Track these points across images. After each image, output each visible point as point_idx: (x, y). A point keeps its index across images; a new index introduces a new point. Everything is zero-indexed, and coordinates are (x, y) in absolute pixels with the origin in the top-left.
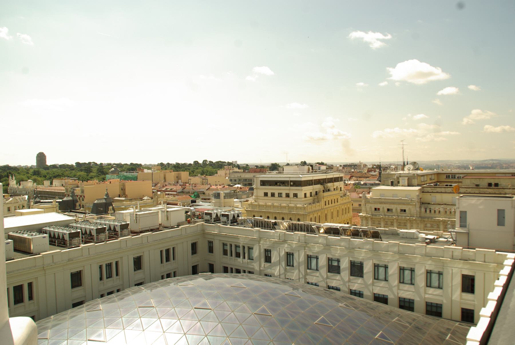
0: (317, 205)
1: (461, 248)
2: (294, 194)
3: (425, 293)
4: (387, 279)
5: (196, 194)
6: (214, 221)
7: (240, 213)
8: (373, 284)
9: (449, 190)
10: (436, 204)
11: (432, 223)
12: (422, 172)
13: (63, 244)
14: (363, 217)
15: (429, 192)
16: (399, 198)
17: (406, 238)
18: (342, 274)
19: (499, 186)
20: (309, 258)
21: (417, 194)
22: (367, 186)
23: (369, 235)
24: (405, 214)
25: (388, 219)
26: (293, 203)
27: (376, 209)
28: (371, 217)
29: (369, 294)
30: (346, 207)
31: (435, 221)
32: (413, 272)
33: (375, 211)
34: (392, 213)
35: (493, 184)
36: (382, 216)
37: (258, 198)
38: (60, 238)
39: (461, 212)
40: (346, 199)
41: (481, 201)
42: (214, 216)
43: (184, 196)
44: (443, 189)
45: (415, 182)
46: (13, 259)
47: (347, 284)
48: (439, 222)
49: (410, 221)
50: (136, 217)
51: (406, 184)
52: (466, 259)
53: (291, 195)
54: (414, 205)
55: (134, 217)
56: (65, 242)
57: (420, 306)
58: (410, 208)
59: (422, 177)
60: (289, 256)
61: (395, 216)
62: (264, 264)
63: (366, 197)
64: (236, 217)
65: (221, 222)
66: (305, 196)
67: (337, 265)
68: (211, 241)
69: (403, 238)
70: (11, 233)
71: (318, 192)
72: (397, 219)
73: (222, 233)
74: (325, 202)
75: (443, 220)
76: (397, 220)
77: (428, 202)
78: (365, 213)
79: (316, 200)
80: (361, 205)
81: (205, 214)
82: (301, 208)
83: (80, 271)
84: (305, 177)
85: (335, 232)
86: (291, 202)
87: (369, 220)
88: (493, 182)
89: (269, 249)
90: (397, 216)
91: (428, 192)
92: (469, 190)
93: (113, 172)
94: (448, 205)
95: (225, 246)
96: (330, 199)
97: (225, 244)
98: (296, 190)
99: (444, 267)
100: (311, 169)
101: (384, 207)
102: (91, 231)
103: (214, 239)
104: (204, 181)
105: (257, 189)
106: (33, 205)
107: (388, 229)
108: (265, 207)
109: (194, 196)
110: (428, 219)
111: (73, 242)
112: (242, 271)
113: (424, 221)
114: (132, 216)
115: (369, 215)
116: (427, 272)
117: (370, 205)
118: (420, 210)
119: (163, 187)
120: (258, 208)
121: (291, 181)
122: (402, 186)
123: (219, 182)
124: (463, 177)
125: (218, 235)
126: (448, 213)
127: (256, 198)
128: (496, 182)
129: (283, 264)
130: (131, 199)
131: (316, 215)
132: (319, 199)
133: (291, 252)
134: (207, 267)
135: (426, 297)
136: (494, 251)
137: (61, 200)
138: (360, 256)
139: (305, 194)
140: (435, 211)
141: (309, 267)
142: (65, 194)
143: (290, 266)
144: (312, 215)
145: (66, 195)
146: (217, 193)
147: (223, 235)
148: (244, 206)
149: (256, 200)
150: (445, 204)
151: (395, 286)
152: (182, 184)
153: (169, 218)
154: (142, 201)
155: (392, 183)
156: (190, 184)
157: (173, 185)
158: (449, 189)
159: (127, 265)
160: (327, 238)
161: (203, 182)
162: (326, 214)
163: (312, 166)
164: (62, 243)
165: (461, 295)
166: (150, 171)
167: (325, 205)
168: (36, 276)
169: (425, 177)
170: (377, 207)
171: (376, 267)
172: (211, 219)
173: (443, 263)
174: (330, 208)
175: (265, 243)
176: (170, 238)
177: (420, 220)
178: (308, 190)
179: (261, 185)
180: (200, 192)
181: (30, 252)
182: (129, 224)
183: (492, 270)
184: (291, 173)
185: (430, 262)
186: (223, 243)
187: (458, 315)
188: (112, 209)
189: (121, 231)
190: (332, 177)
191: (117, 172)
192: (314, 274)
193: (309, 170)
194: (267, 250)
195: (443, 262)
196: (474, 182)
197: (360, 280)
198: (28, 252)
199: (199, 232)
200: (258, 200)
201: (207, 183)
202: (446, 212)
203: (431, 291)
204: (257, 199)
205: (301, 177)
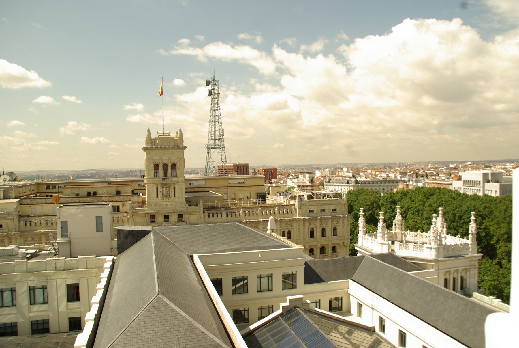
1: (64, 258)
3: (30, 312)
9: (50, 200)
10: (37, 216)
11: (33, 236)
12: (19, 182)
15: (29, 203)
17: (4, 256)
21: (15, 206)
24: (2, 229)
31: (36, 234)
35: (92, 192)
41: (80, 210)
44: (43, 200)
45: (12, 193)
48: (41, 234)
49: (8, 237)
52: (69, 269)
54: (12, 219)
58: (7, 223)
59: (21, 189)
75: (44, 232)
88: (92, 191)
92: (70, 200)
94: (49, 216)
110: (28, 232)
116: (30, 289)
126: (50, 224)
135: (30, 315)
136: (95, 256)
140: (36, 223)
150: (46, 216)
165: (67, 306)
169: (24, 188)
173: (47, 277)
177: (19, 234)
183: (94, 275)
185: (32, 278)
187: (65, 325)
195: (47, 276)
196: (74, 191)
202: (47, 223)
203: (35, 308)
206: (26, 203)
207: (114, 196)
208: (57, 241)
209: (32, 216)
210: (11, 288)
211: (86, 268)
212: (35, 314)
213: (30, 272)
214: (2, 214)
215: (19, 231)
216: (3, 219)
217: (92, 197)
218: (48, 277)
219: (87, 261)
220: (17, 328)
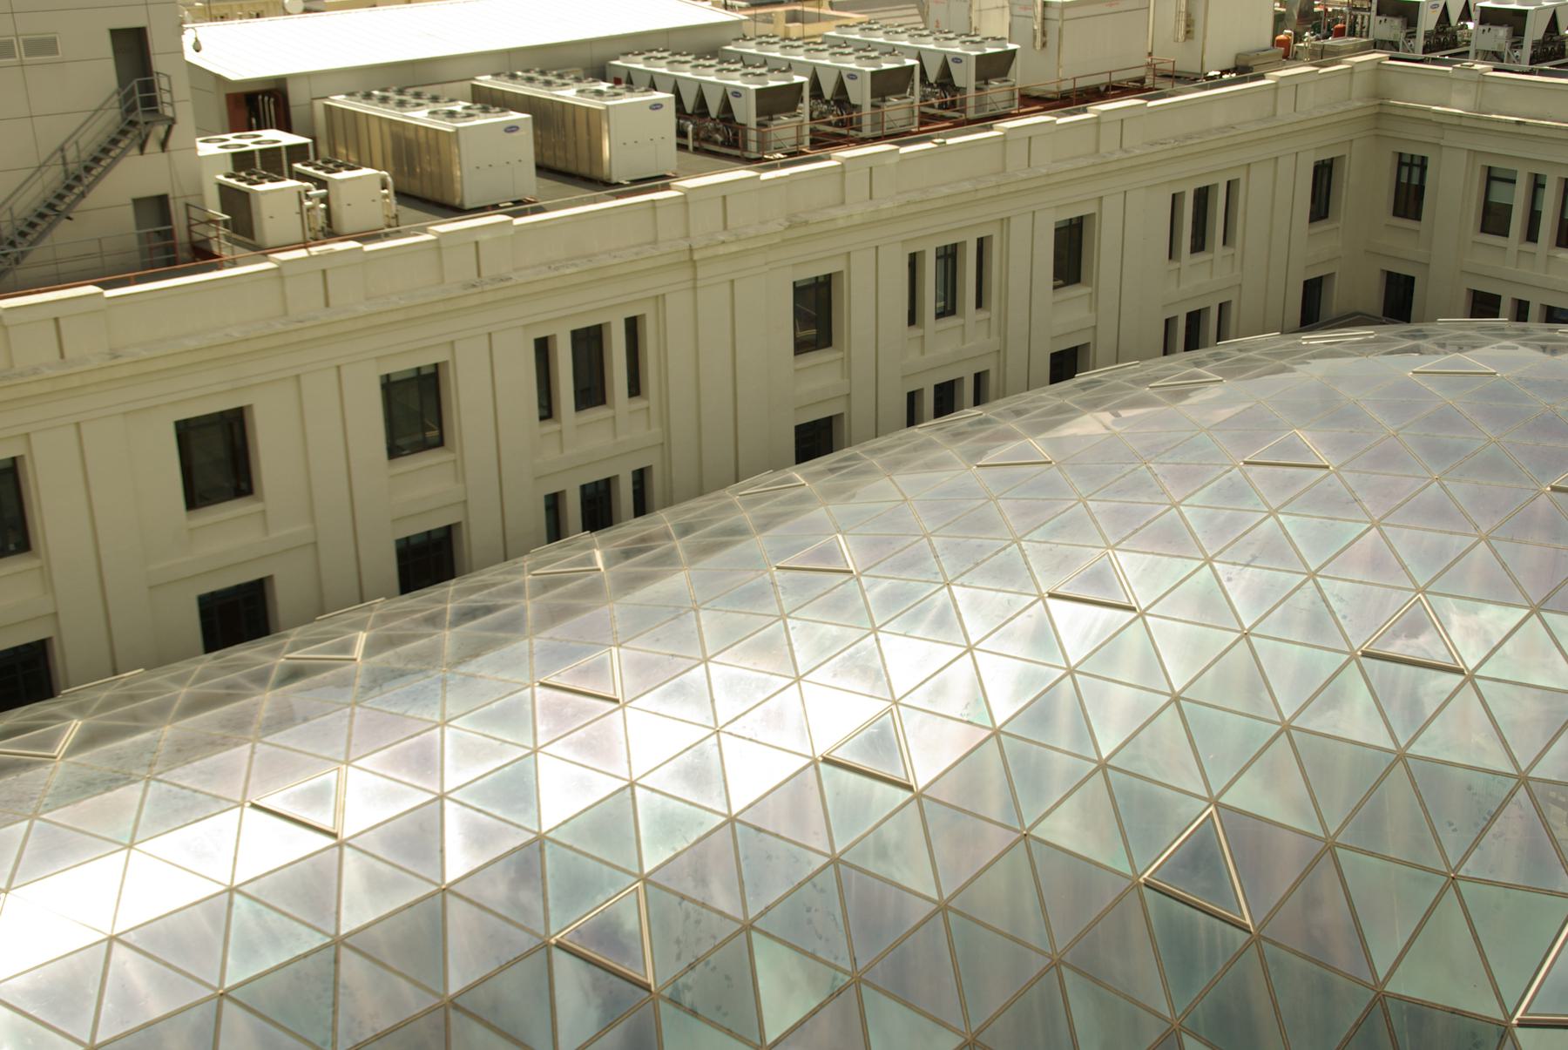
13: (723, 144)
46: (540, 210)
50: (1044, 19)
55: (1036, 17)
56: (735, 134)
65: (1472, 53)
68: (1412, 156)
70: (486, 81)
73: (1494, 116)
83: (829, 277)
95: (1497, 187)
97: (1495, 174)
102: (847, 82)
103: (1441, 146)
111: (773, 138)
114: (1017, 11)
125: (1464, 122)
134: (1373, 296)
153: (1198, 29)
164: (719, 138)
168: (660, 292)
176: (1220, 129)
181: (596, 174)
182: (1014, 52)
186: (1490, 168)
198: (596, 182)
199: (1359, 104)
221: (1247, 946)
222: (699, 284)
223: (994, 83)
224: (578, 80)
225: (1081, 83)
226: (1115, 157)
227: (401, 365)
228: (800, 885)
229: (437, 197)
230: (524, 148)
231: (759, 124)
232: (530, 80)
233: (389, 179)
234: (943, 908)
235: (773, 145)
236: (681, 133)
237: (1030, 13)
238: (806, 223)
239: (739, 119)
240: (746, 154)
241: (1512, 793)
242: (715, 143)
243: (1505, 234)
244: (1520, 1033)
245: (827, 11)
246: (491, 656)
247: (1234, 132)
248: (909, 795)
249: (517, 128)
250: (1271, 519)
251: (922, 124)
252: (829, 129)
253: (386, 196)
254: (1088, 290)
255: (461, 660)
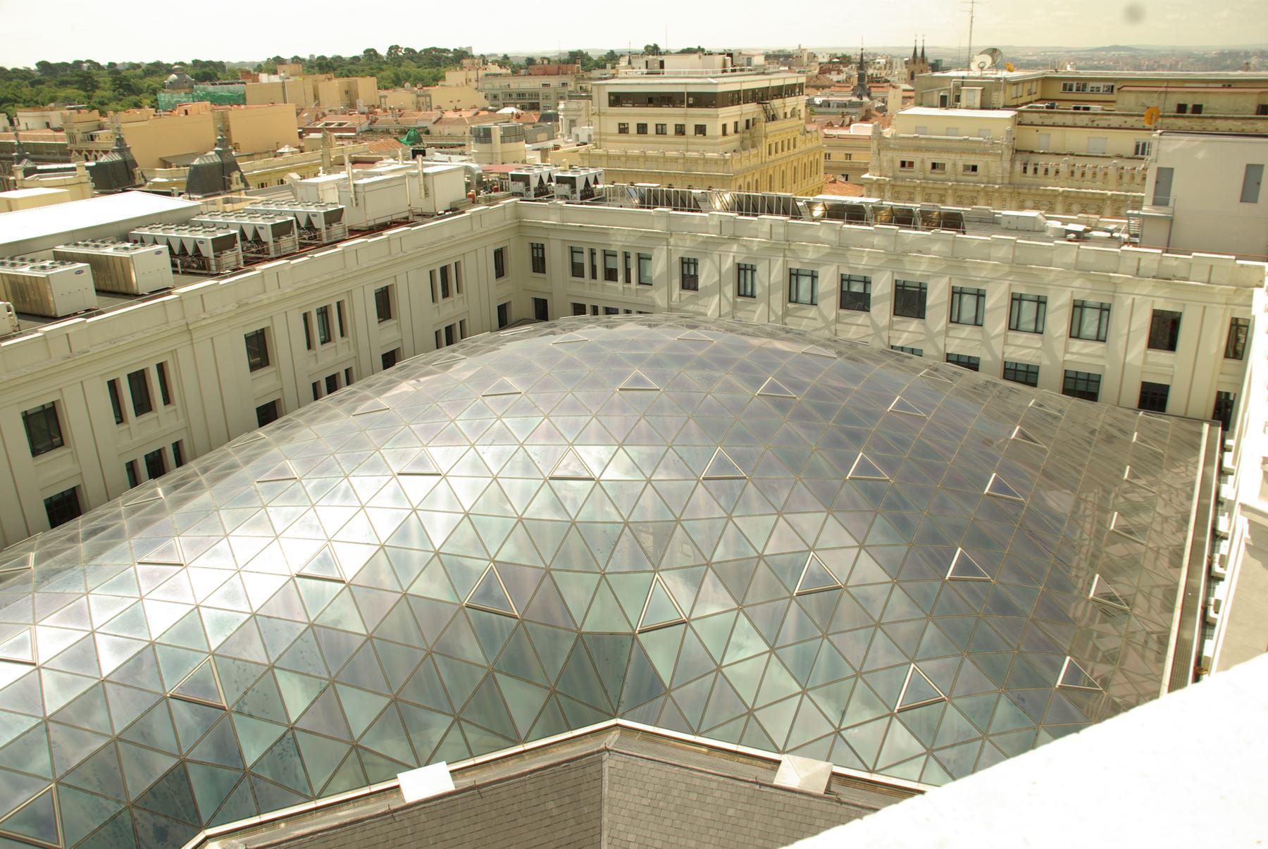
0: (752, 153)
1: (1160, 251)
2: (676, 125)
3: (1066, 352)
4: (980, 322)
5: (412, 133)
6: (536, 195)
7: (600, 174)
8: (946, 333)
9: (1084, 119)
11: (1037, 198)
12: (1010, 73)
13: (197, 268)
14: (872, 184)
15: (1035, 123)
16: (962, 138)
17: (1017, 229)
18: (874, 309)
19: (1203, 112)
20: (794, 275)
21: (1008, 128)
22: (830, 110)
23: (933, 222)
24: (976, 175)
25: (933, 188)
26: (695, 148)
27: (903, 164)
28: (893, 183)
29: (933, 352)
30: (811, 158)
31: (1045, 194)
32: (1042, 306)
33: (902, 169)
34: (944, 174)
35: (1190, 106)
36: (918, 181)
37: (603, 137)
38: (187, 254)
39: (1159, 170)
40: (811, 140)
42: (534, 183)
43: (382, 140)
45: (999, 98)
47: (885, 335)
48: (1056, 196)
50: (355, 192)
51: (977, 102)
52: (1166, 277)
53: (690, 130)
56: (203, 263)
57: (1051, 377)
58: (987, 162)
59: (1015, 87)
60: (744, 271)
61: (949, 180)
62: (680, 295)
63: (881, 133)
64: (591, 181)
66: (724, 133)
67: (862, 291)
69: (1007, 228)
70: (61, 248)
71: (751, 122)
72: (954, 187)
74: (770, 145)
75: (1063, 191)
76: (956, 190)
77: (1030, 149)
78: (878, 174)
79: (748, 142)
80: (850, 155)
81: (510, 178)
82: (716, 161)
84: (725, 83)
85: (855, 214)
86: (690, 147)
87: (886, 191)
88: (1190, 102)
89: (692, 256)
90: (956, 181)
91: (1032, 124)
93: (174, 86)
94: (1077, 155)
96: (778, 139)
98: (704, 116)
99: (1116, 294)
100: (729, 64)
101: (923, 160)
102: (259, 231)
104: (422, 99)
105: (599, 115)
106: (22, 180)
107: (970, 209)
108: (623, 159)
109: (408, 140)
110: (1029, 189)
112: (621, 310)
113: (1019, 193)
114: (341, 189)
115: (888, 179)
116: (1075, 306)
117: (890, 154)
118: (1012, 166)
119: (317, 119)
120: (604, 163)
121: (689, 94)
122: (967, 108)
123: (459, 101)
124: (1119, 89)
125: (557, 227)
126: (1078, 174)
127: (598, 137)
128: (1197, 103)
129: (726, 291)
130: (253, 155)
131: (749, 179)
132: (755, 139)
133: (749, 262)
134: (530, 311)
135: (1065, 358)
136: (1233, 257)
137: (92, 164)
138: (916, 271)
139: (724, 126)
140: (1046, 170)
141: (794, 298)
142: (68, 148)
143: (745, 295)
144: (742, 179)
145: (71, 151)
146: (482, 130)
147: (574, 229)
148: (565, 160)
149: (598, 143)
150: (1072, 154)
151: (997, 336)
152: (366, 110)
154: (280, 159)
155: (943, 99)
156: (385, 110)
157: (343, 114)
158: (1083, 116)
159: (363, 309)
160: (841, 231)
161: (418, 102)
162: (771, 176)
163: (730, 55)
164: (195, 266)
165: (1146, 355)
166: (275, 79)
167: (770, 154)
168: (174, 348)
169: (1020, 86)
170: (907, 159)
171: (957, 293)
172: (528, 190)
173: (1115, 285)
174: (780, 162)
175: (680, 243)
176: (448, 238)
177: (1009, 190)
178: (730, 115)
179: (611, 105)
180: (419, 128)
181: (130, 291)
182: (342, 209)
183: (1223, 301)
184: (684, 73)
185: (1078, 283)
187: (1133, 394)
188: (240, 180)
189: (327, 229)
190: (780, 83)
191: (186, 85)
192: (804, 311)
193: (724, 65)
194: (686, 261)
196: (1144, 101)
197: (913, 325)
200: (602, 143)
201: (431, 106)
202: (1073, 173)
203: (1077, 345)
204: (600, 140)
205: (716, 84)
206: (1029, 123)
207: (1250, 119)
208: (1141, 213)
209: (1039, 153)
210: (1039, 296)
211: (1206, 280)
212: (1074, 358)
213: (1080, 269)
214: (980, 142)
215: (1010, 184)
216: (981, 154)
217: (1189, 117)
218: (1116, 287)
219: (1211, 266)
220: (1037, 377)
221: (518, 625)
222: (194, 341)
223: (335, 225)
224: (113, 243)
225: (378, 222)
226: (401, 255)
227: (33, 405)
228: (295, 641)
229: (41, 312)
230: (88, 281)
231: (215, 256)
232: (87, 245)
233: (12, 306)
234: (370, 638)
235: (224, 266)
236: (174, 265)
237: (348, 190)
238: (247, 304)
239: (204, 254)
240: (211, 272)
241: (623, 531)
242: (193, 268)
243: (583, 277)
244: (640, 637)
245: (244, 196)
246: (108, 553)
247: (454, 239)
248: (343, 585)
249: (82, 272)
250: (499, 421)
251: (301, 248)
252: (253, 255)
253: (11, 315)
254: (396, 321)
255: (92, 558)
